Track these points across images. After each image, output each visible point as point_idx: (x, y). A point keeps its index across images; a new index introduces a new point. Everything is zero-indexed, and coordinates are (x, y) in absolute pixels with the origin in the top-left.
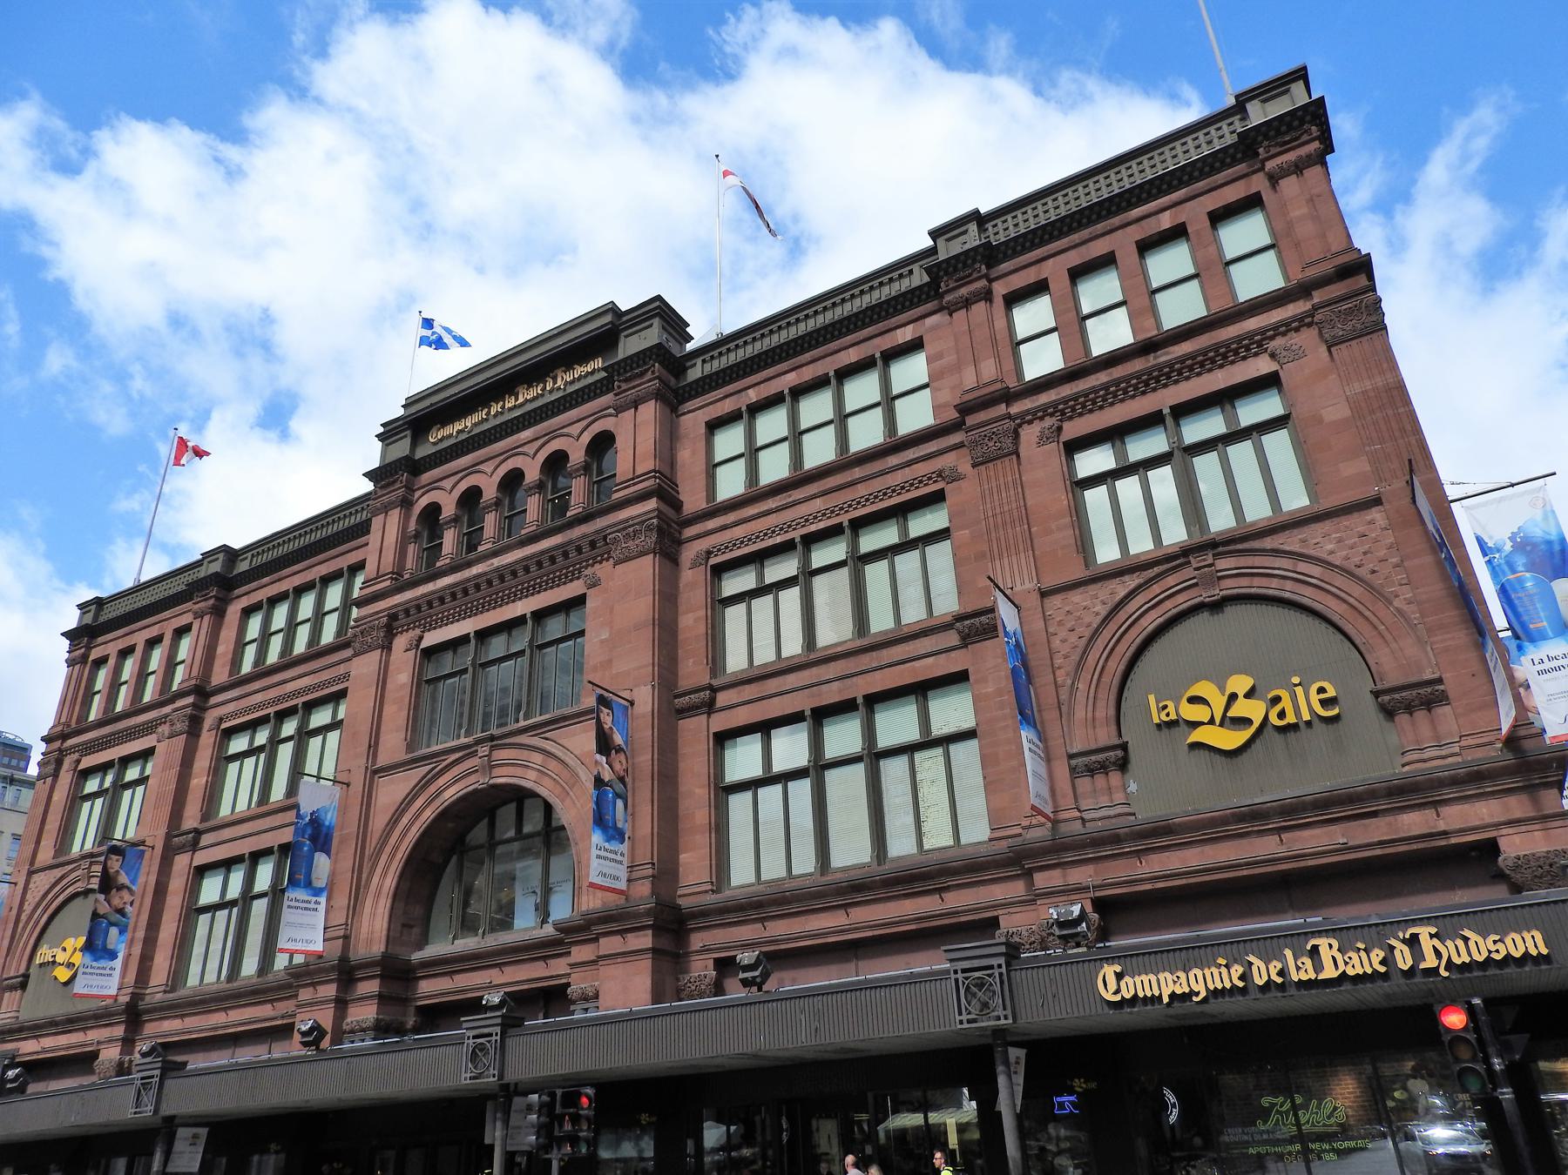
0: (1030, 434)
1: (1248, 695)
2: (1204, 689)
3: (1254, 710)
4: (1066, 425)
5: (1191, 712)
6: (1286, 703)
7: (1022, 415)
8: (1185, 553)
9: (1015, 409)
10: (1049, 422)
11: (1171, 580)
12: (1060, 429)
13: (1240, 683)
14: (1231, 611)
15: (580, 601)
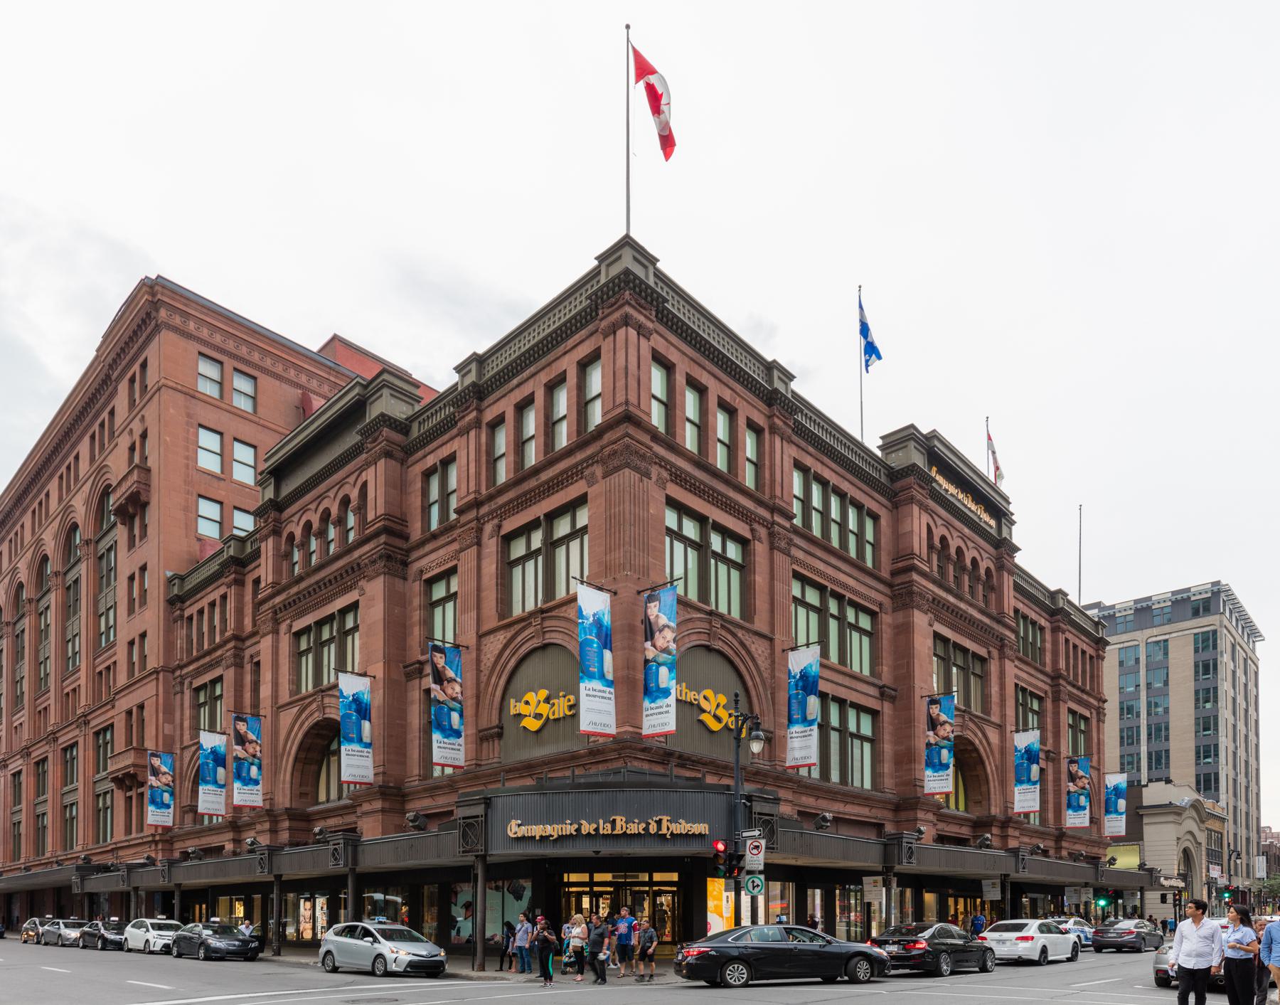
0: (488, 528)
1: (547, 700)
2: (530, 696)
3: (544, 709)
4: (504, 523)
5: (522, 708)
6: (556, 707)
7: (483, 516)
8: (532, 614)
9: (484, 510)
10: (496, 521)
11: (527, 632)
12: (499, 527)
13: (544, 693)
14: (550, 651)
15: (354, 607)
